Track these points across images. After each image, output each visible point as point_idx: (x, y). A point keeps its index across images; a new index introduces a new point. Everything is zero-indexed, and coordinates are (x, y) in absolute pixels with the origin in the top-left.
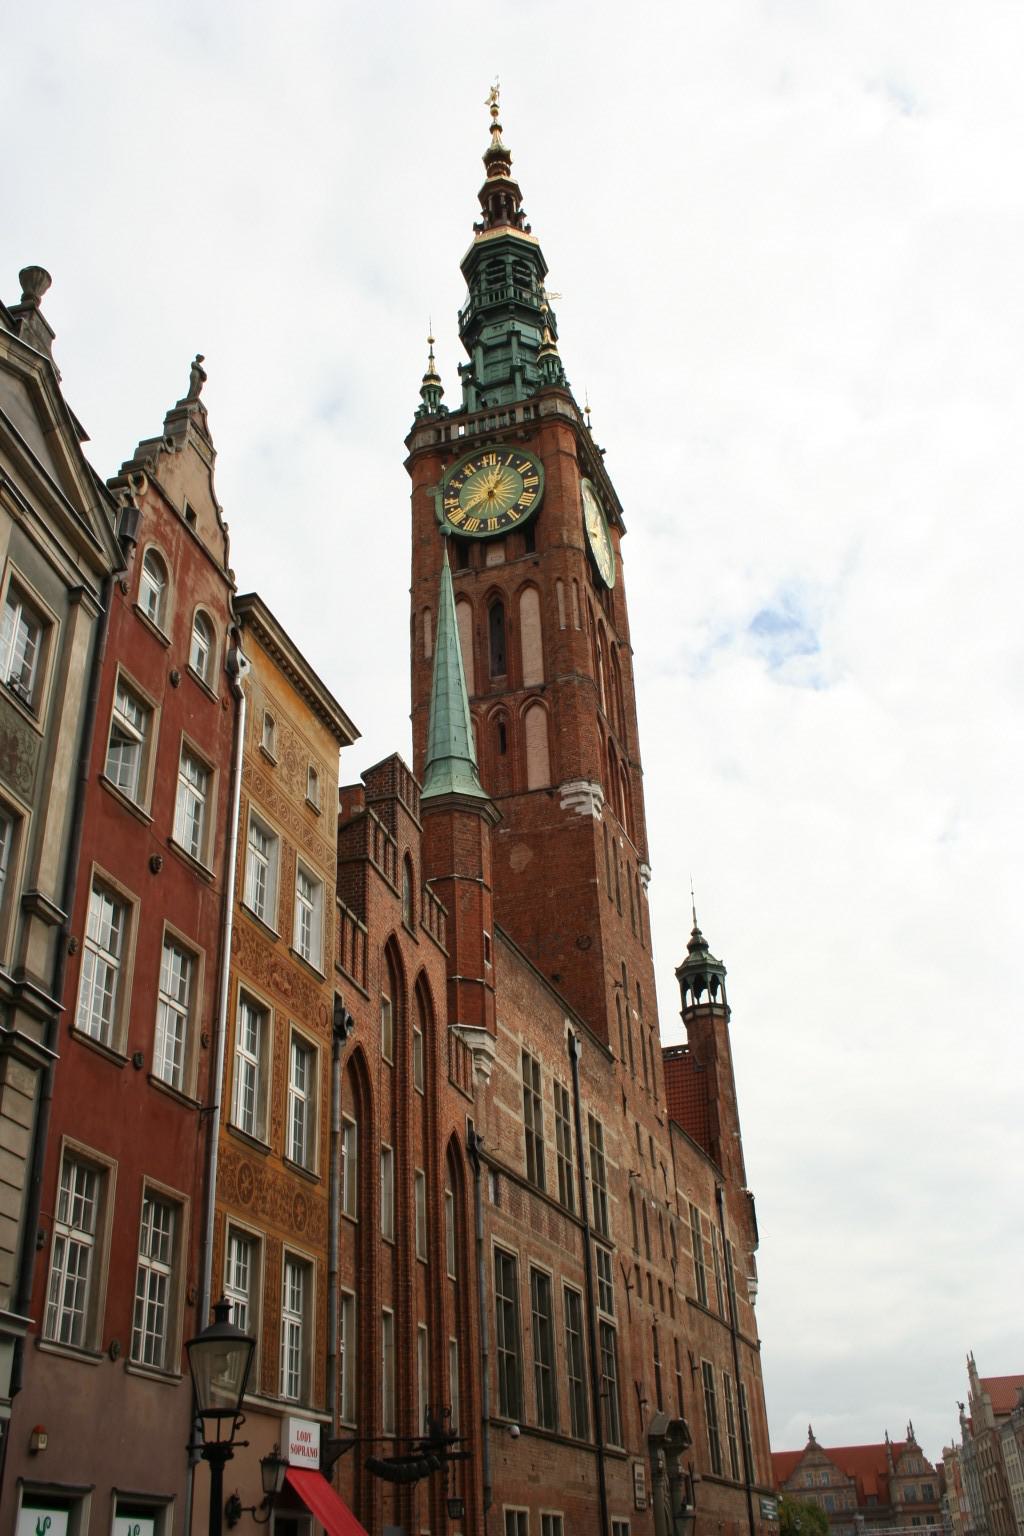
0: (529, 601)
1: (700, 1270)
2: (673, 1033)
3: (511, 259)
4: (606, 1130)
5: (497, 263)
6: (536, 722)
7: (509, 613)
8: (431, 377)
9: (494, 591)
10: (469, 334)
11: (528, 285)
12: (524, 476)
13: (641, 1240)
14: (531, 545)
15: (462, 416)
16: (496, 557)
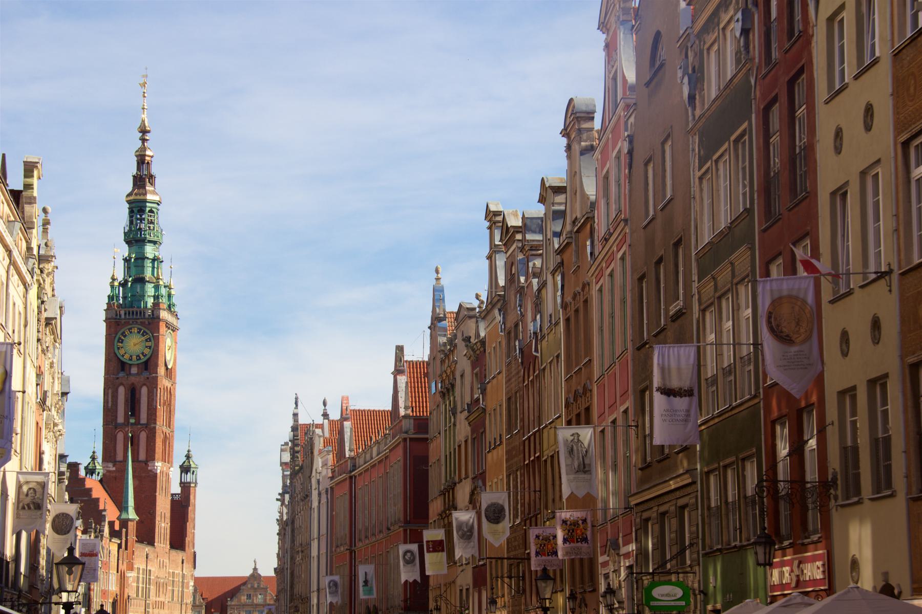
0: (144, 390)
1: (173, 591)
2: (176, 489)
3: (148, 209)
4: (153, 569)
5: (142, 211)
6: (143, 436)
7: (137, 396)
8: (113, 279)
9: (133, 384)
10: (129, 242)
11: (153, 223)
12: (146, 340)
13: (158, 594)
14: (146, 369)
15: (124, 284)
16: (134, 370)
